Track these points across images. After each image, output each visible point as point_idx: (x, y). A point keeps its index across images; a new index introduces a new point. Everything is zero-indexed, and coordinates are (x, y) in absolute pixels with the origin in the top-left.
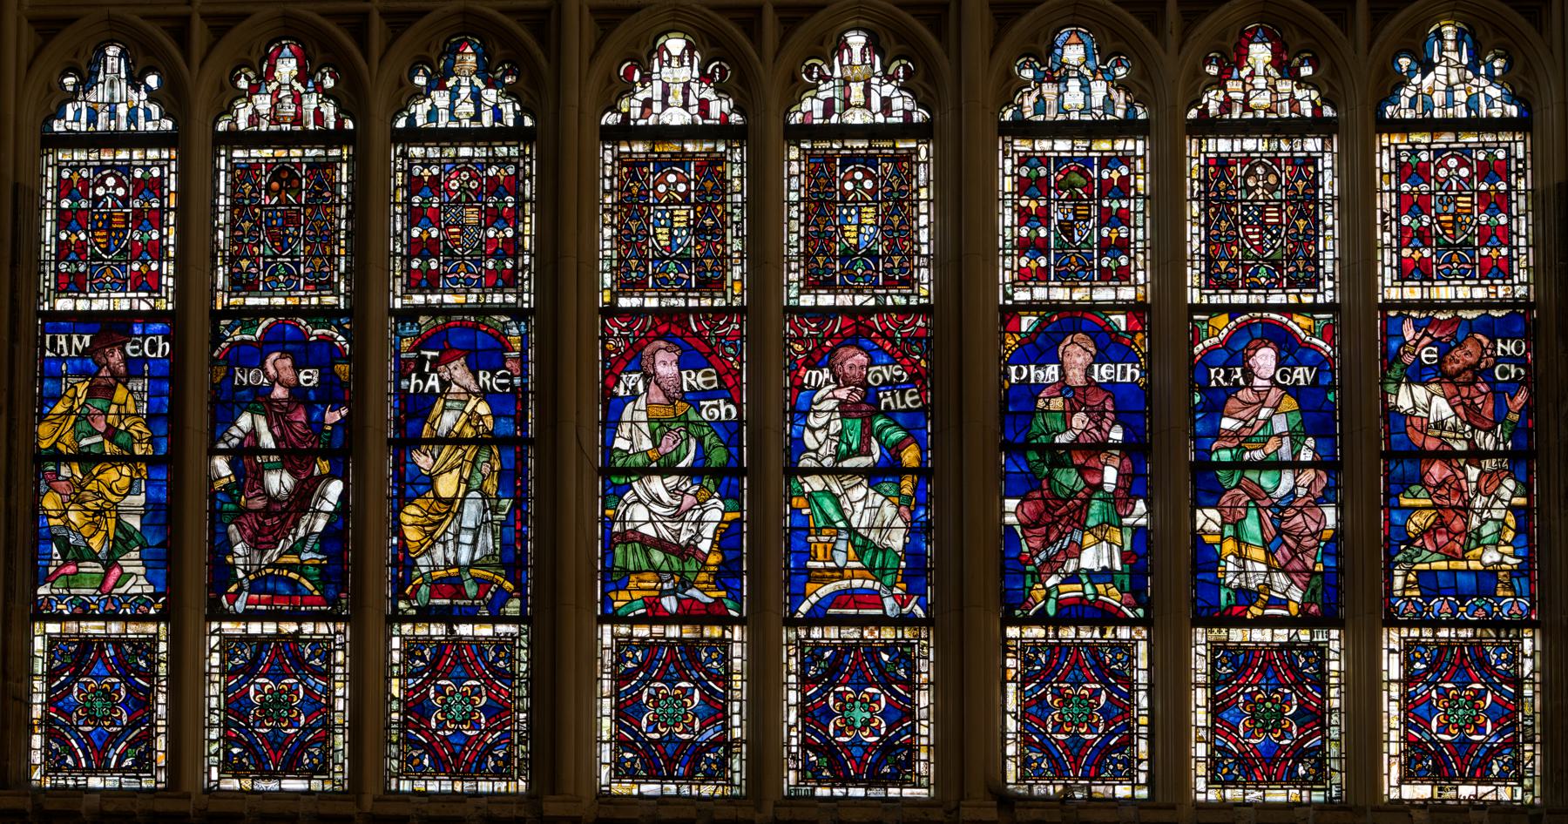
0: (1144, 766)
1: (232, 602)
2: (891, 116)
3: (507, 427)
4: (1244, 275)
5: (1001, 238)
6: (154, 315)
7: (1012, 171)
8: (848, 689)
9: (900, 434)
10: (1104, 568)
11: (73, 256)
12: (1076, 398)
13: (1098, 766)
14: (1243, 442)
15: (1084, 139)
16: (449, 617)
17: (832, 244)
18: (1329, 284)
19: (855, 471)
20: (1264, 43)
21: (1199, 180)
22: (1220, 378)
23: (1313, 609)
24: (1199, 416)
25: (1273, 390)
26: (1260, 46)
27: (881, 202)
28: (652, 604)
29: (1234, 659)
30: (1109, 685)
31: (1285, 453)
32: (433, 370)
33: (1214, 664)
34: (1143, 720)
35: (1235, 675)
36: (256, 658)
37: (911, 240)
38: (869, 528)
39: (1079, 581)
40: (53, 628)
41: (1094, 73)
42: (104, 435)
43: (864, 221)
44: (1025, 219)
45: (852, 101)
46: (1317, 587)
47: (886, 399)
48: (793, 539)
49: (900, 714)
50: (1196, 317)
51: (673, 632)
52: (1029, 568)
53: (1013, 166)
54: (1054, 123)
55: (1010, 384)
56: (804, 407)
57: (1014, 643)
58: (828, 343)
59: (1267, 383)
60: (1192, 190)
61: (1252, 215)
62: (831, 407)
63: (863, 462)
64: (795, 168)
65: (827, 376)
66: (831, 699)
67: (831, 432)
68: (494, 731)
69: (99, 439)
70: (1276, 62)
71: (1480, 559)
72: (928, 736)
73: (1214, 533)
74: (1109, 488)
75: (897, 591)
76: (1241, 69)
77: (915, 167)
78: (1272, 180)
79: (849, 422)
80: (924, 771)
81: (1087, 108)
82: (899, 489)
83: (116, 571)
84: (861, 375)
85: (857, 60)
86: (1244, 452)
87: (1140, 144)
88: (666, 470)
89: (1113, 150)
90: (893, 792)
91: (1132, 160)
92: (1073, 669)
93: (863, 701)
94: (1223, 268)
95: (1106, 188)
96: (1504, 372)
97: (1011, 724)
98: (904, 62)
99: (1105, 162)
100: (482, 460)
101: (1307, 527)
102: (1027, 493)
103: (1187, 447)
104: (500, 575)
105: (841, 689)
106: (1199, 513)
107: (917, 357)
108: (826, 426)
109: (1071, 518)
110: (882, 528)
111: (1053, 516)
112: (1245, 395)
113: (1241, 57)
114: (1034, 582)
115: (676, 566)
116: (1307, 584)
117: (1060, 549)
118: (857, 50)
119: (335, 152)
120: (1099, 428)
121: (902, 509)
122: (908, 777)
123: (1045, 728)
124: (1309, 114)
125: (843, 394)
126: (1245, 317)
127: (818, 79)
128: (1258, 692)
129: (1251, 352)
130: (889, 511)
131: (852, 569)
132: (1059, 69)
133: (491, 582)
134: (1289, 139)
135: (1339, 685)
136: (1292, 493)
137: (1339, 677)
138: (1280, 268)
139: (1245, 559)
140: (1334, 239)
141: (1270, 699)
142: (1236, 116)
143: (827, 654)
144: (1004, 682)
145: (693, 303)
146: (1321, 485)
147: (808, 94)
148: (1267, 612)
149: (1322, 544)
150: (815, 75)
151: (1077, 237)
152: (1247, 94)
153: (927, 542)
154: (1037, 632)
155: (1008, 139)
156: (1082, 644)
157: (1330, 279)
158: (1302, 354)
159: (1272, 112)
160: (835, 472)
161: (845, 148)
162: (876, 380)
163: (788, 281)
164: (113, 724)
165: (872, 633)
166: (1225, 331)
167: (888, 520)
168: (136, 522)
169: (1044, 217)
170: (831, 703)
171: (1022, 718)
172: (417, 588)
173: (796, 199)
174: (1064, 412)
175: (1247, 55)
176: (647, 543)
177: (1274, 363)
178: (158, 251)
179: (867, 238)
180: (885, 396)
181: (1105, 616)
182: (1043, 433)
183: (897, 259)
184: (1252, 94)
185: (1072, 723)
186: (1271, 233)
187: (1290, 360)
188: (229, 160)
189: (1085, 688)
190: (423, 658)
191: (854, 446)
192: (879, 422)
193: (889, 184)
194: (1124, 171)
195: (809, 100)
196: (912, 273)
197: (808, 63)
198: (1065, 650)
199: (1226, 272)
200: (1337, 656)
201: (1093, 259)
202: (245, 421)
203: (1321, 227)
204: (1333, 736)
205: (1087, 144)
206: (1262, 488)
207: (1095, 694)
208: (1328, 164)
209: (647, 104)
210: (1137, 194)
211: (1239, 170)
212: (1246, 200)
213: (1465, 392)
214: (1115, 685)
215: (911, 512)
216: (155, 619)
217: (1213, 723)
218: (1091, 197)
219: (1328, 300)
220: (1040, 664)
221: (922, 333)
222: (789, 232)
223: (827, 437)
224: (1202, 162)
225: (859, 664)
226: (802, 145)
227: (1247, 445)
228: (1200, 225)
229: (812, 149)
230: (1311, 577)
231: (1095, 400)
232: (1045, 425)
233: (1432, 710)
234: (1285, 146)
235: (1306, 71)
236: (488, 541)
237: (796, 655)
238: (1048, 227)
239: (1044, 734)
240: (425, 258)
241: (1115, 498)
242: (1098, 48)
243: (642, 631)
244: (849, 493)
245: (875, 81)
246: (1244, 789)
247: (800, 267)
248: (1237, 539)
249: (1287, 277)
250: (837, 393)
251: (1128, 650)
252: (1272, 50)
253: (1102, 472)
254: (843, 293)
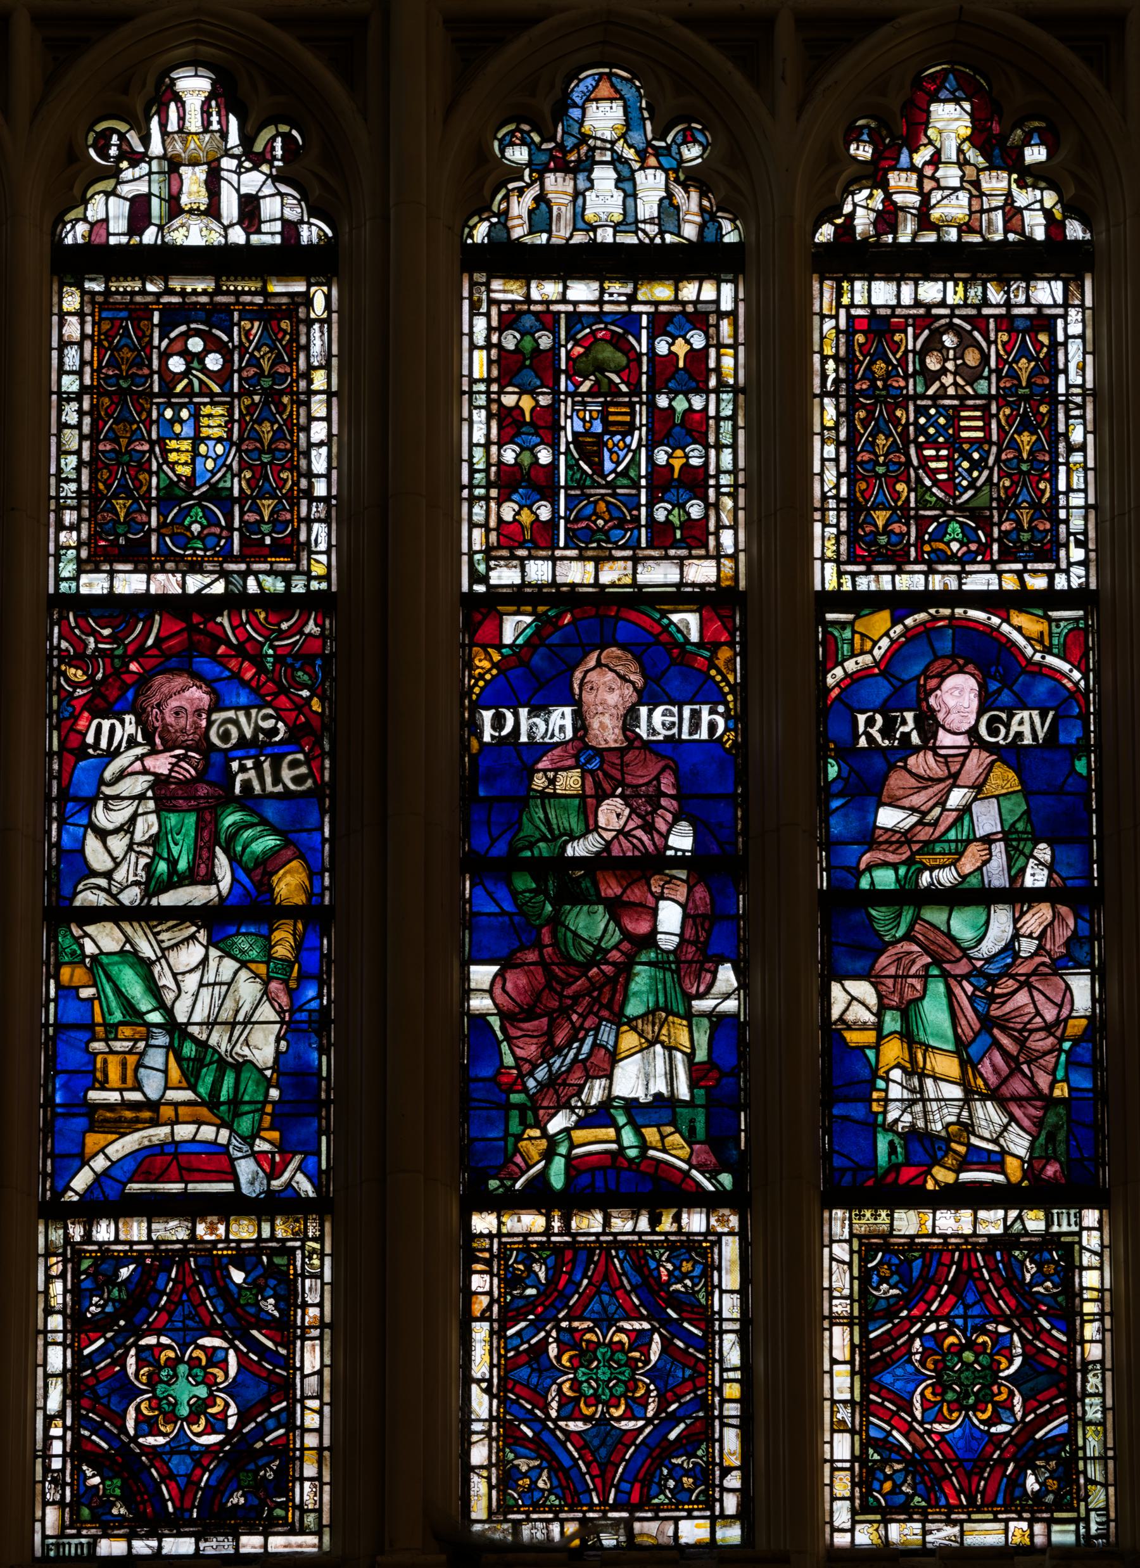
0: (734, 1481)
2: (259, 232)
4: (920, 536)
5: (465, 466)
7: (488, 338)
8: (164, 1340)
9: (270, 842)
10: (658, 1096)
13: (647, 1483)
14: (918, 852)
15: (623, 280)
17: (143, 477)
18: (1077, 554)
20: (957, 101)
21: (836, 358)
22: (874, 732)
23: (1050, 1170)
24: (835, 804)
25: (974, 754)
26: (950, 107)
27: (239, 396)
29: (903, 1272)
30: (666, 1322)
31: (997, 874)
33: (864, 1278)
34: (732, 1391)
35: (905, 1300)
37: (294, 468)
38: (210, 1024)
39: (612, 1123)
41: (642, 155)
43: (205, 432)
44: (510, 431)
45: (184, 200)
46: (1057, 1127)
47: (243, 774)
48: (61, 1047)
49: (264, 1387)
50: (830, 616)
52: (515, 1098)
53: (490, 329)
54: (567, 248)
55: (482, 744)
56: (87, 791)
57: (486, 1243)
58: (134, 667)
59: (962, 740)
60: (824, 377)
61: (935, 424)
62: (137, 790)
63: (198, 895)
64: (73, 329)
65: (131, 729)
66: (131, 1361)
67: (139, 837)
70: (979, 137)
72: (319, 1431)
73: (864, 1027)
74: (668, 942)
75: (261, 1146)
76: (914, 149)
77: (303, 329)
78: (972, 358)
79: (173, 819)
80: (309, 1500)
81: (628, 222)
82: (268, 947)
84: (197, 726)
85: (194, 123)
86: (920, 872)
87: (727, 289)
89: (676, 301)
90: (251, 1544)
91: (712, 320)
92: (599, 1292)
93: (194, 1363)
94: (880, 523)
97: (481, 1404)
98: (284, 128)
99: (661, 324)
101: (1038, 1013)
102: (513, 952)
103: (814, 862)
105: (151, 1340)
106: (836, 989)
107: (305, 693)
108: (128, 827)
109: (596, 1000)
110: (233, 1024)
111: (561, 996)
112: (922, 763)
114: (525, 1125)
116: (1039, 1123)
117: (575, 1060)
118: (194, 104)
120: (649, 828)
121: (274, 986)
122: (279, 1512)
123: (545, 1408)
124: (1040, 234)
125: (161, 764)
126: (922, 616)
127: (119, 159)
128: (949, 1332)
129: (933, 683)
130: (248, 990)
131: (176, 1105)
132: (576, 147)
134: (1004, 283)
135: (1101, 1317)
136: (1010, 948)
137: (1101, 1300)
138: (986, 524)
139: (922, 1076)
140: (1086, 469)
141: (970, 1345)
142: (904, 238)
143: (125, 1273)
144: (466, 1321)
146: (1063, 934)
147: (99, 186)
148: (965, 1176)
149: (1067, 1045)
150: (113, 151)
151: (608, 466)
152: (925, 197)
153: (322, 1050)
154: (532, 1222)
155: (480, 277)
156: (616, 1244)
157: (1079, 544)
158: (1027, 687)
159: (971, 230)
161: (170, 292)
162: (225, 737)
163: (58, 547)
165: (212, 1229)
166: (885, 643)
167: (246, 1008)
170: (131, 1370)
171: (499, 1392)
173: (75, 388)
174: (582, 797)
175: (926, 124)
177: (975, 704)
179: (210, 464)
180: (243, 769)
182: (544, 839)
183: (267, 506)
184: (936, 196)
185: (595, 1400)
186: (969, 458)
187: (1006, 697)
189: (621, 1330)
191: (182, 865)
192: (231, 819)
193: (255, 362)
194: (698, 341)
195: (100, 198)
196: (296, 532)
197: (99, 128)
198: (583, 1256)
199: (886, 531)
200: (1095, 1261)
201: (638, 506)
203: (1062, 447)
204: (1090, 1416)
205: (629, 289)
206: (954, 939)
207: (641, 1340)
208: (1075, 329)
210: (722, 385)
211: (910, 340)
212: (924, 397)
214: (678, 1323)
215: (291, 993)
217: (864, 1394)
218: (635, 390)
219: (1075, 583)
220: (537, 1284)
221: (315, 647)
222: (61, 452)
223: (130, 848)
224: (843, 324)
225: (186, 1290)
226: (88, 285)
227: (926, 859)
228: (839, 444)
229: (107, 293)
230: (1046, 1109)
231: (641, 774)
232: (547, 822)
234: (995, 296)
235: (1035, 154)
237: (62, 1276)
238: (554, 446)
239: (543, 1422)
241: (678, 962)
242: (649, 108)
244: (172, 956)
245: (228, 163)
246: (924, 1522)
247: (80, 519)
248: (908, 1037)
249: (999, 540)
250: (150, 762)
251: (704, 1253)
252: (972, 115)
253: (655, 912)
254: (163, 571)
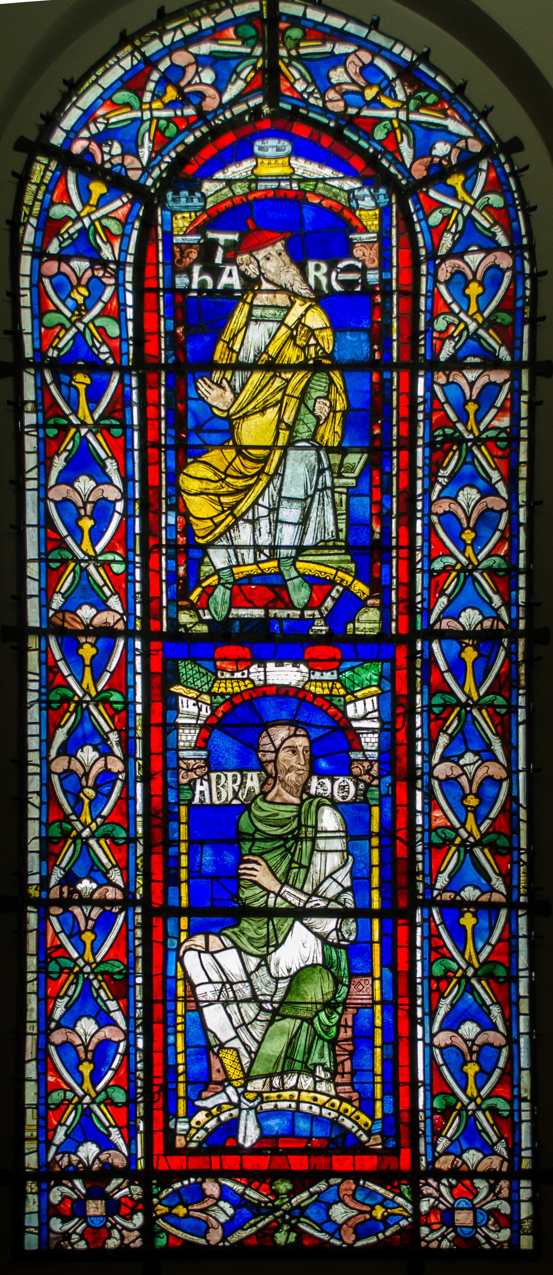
32: (229, 260)
100: (314, 395)
104: (347, 571)
133: (332, 583)
172: (209, 592)
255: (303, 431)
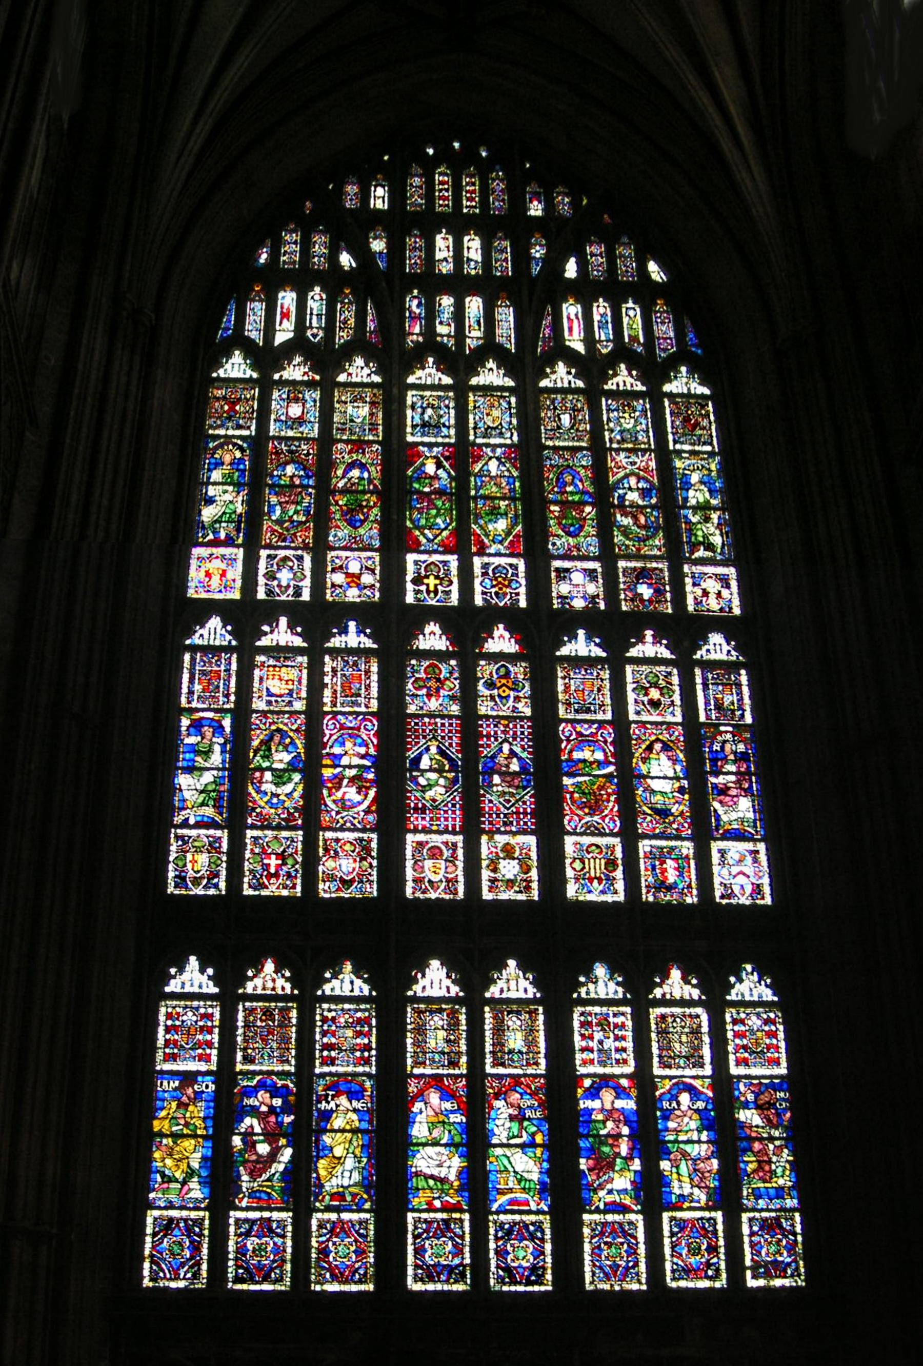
1: (241, 1200)
3: (365, 1125)
6: (208, 1073)
11: (172, 1046)
12: (610, 1114)
16: (338, 1210)
19: (516, 1146)
28: (429, 1203)
31: (695, 1138)
32: (332, 1099)
36: (251, 1228)
40: (156, 1213)
42: (183, 1125)
51: (439, 1216)
68: (358, 1262)
69: (181, 1127)
71: (776, 1182)
83: (186, 1188)
85: (513, 971)
88: (435, 1143)
95: (616, 1026)
96: (781, 1105)
99: (615, 1015)
113: (668, 976)
115: (440, 1187)
119: (290, 1005)
145: (445, 1072)
154: (596, 1217)
160: (508, 1146)
164: (182, 1258)
168: (195, 1165)
169: (591, 1037)
172: (324, 1197)
176: (427, 1177)
178: (210, 1044)
181: (623, 1209)
188: (244, 1006)
190: (326, 1228)
192: (526, 1123)
202: (248, 1121)
209: (424, 988)
213: (766, 1112)
216: (204, 1209)
233: (762, 1247)
236: (356, 1177)
240: (329, 1051)
243: (424, 1216)
255: (351, 1151)
